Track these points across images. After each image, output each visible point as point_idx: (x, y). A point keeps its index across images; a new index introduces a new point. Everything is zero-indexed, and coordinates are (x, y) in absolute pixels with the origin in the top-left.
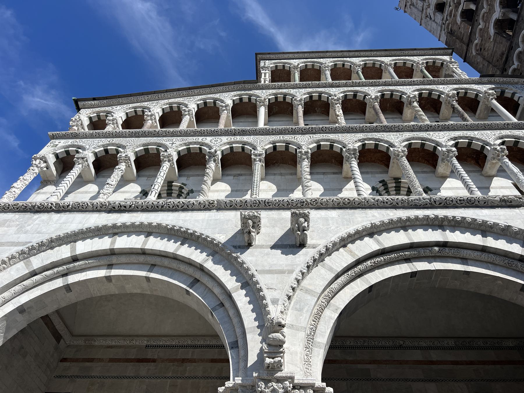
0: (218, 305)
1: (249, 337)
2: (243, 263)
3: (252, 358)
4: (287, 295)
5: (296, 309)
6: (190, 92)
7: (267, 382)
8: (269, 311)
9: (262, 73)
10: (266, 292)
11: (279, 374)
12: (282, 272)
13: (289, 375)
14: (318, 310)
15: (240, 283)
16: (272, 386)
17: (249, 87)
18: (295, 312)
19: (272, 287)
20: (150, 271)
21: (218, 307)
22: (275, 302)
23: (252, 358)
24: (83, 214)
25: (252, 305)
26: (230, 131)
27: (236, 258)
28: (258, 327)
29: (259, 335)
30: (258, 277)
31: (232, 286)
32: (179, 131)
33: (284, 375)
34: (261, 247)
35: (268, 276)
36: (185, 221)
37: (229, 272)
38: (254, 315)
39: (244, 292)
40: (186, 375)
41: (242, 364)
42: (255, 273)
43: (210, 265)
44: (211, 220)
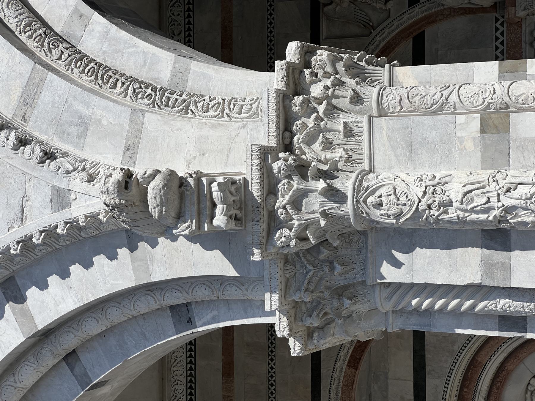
0: (72, 369)
4: (42, 162)
5: (83, 135)
8: (86, 217)
11: (255, 189)
13: (256, 161)
14: (82, 72)
15: (7, 307)
16: (284, 208)
18: (89, 139)
19: (18, 208)
21: (77, 370)
28: (133, 248)
29: (154, 244)
31: (16, 329)
33: (257, 174)
38: (100, 260)
39: (32, 293)
41: (233, 293)
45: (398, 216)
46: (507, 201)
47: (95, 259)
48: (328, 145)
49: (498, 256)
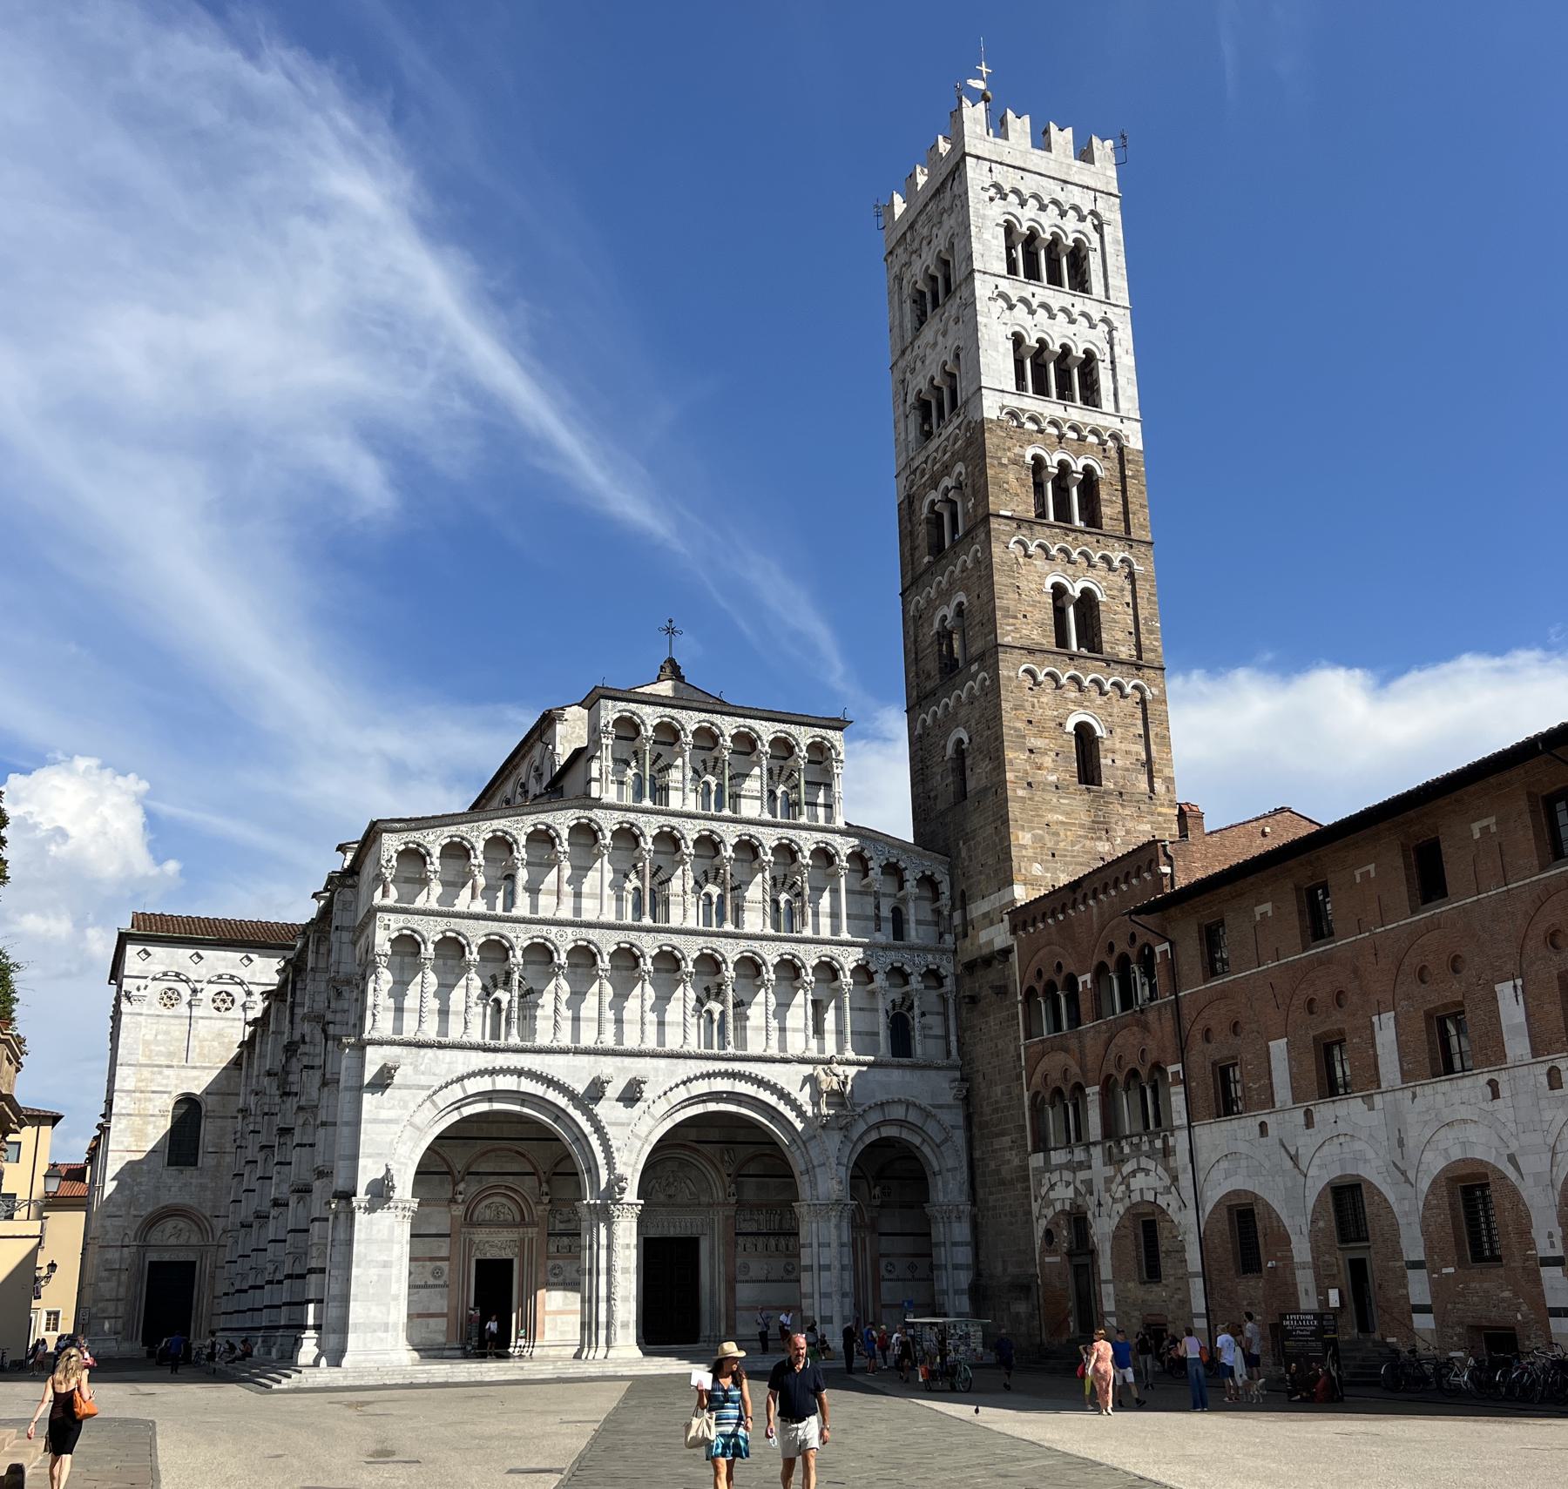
1: (601, 1171)
2: (597, 1115)
3: (603, 1185)
7: (615, 1205)
12: (622, 1124)
20: (522, 1105)
23: (603, 1185)
34: (609, 1099)
35: (614, 1128)
36: (549, 1066)
39: (596, 1136)
41: (595, 1187)
42: (606, 1126)
43: (571, 1110)
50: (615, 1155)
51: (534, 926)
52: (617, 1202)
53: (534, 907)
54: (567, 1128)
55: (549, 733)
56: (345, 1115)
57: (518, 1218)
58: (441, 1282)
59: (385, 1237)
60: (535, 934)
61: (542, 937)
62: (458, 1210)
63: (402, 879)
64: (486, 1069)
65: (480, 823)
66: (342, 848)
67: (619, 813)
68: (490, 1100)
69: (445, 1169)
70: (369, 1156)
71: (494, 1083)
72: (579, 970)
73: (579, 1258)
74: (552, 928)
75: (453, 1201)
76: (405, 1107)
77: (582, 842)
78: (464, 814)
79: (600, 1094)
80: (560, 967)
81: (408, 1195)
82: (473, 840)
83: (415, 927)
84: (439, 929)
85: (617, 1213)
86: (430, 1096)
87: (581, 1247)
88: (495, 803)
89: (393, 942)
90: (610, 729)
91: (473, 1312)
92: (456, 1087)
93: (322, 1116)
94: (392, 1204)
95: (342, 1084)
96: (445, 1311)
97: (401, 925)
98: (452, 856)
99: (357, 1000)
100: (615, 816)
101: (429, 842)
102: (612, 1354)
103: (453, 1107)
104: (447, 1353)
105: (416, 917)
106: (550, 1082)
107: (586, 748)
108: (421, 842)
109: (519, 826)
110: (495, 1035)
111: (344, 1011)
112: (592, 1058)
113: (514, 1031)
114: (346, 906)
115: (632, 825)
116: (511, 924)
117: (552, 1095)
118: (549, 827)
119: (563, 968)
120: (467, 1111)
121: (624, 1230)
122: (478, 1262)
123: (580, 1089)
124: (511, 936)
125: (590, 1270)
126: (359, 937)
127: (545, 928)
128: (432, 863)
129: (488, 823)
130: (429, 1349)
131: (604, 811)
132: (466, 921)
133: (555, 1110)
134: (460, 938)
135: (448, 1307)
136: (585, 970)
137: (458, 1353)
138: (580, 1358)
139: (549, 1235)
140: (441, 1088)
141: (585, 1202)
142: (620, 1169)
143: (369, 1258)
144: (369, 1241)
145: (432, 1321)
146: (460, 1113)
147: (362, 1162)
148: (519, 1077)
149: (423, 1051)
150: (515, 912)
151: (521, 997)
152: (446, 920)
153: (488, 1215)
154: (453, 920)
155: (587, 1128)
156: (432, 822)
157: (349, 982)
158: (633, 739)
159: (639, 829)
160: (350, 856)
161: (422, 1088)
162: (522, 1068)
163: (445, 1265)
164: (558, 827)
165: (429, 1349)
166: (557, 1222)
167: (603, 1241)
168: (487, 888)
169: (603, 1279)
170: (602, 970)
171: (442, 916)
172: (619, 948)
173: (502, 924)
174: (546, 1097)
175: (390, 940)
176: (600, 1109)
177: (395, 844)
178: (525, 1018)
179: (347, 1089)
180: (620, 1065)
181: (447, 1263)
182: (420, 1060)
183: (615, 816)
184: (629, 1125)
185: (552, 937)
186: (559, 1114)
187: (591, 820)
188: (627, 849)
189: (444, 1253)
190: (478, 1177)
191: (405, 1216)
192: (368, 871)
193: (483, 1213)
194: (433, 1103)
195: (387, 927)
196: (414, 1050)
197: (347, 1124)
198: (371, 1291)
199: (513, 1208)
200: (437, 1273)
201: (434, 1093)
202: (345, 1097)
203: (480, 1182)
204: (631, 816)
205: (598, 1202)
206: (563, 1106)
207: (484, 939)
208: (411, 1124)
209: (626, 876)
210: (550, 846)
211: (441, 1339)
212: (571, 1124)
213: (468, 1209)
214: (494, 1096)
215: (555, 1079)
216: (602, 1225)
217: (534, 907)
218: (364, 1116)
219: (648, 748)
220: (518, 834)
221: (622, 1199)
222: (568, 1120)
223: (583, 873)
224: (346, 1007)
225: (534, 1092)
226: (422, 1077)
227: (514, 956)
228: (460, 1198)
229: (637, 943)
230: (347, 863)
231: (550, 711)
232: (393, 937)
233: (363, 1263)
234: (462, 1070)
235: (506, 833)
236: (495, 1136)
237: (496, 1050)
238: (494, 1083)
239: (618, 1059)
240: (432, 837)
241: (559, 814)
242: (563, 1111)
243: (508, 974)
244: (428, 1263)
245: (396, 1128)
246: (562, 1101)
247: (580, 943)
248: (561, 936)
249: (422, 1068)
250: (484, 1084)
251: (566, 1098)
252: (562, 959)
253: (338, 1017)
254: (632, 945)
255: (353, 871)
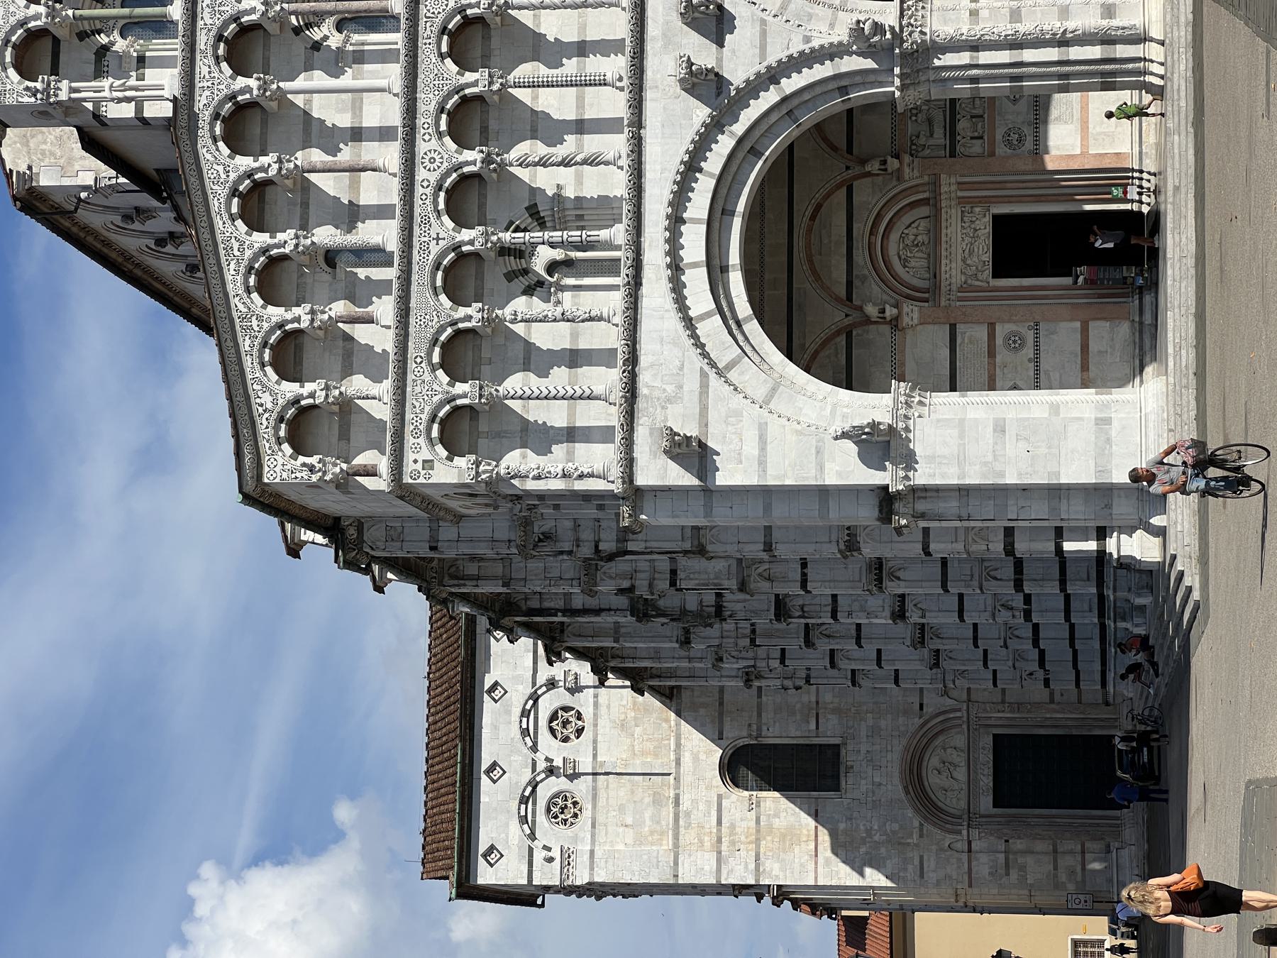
0: (790, 117)
1: (844, 69)
2: (748, 81)
3: (869, 64)
6: (207, 248)
7: (902, 41)
9: (70, 98)
10: (794, 50)
11: (897, 29)
12: (764, 34)
13: (898, 20)
15: (771, 87)
17: (186, 117)
18: (813, 21)
19: (786, 44)
20: (733, 213)
21: (793, 118)
22: (807, 40)
23: (869, 64)
24: (641, 322)
25: (803, 70)
26: (407, 135)
27: (737, 89)
29: (842, 58)
30: (772, 60)
32: (403, 231)
33: (898, 25)
34: (719, 60)
37: (752, 102)
39: (784, 81)
40: (757, 267)
41: (872, 78)
42: (765, 64)
43: (739, 128)
44: (663, 134)
45: (945, 39)
46: (982, 33)
47: (803, 70)
48: (916, 20)
49: (975, 54)
50: (815, 44)
51: (417, 211)
52: (898, 37)
53: (382, 212)
54: (770, 133)
55: (58, 199)
56: (753, 516)
57: (925, 211)
58: (1030, 336)
59: (955, 432)
60: (430, 208)
61: (436, 196)
62: (911, 313)
63: (343, 443)
64: (671, 280)
65: (235, 314)
66: (294, 550)
67: (198, 63)
68: (725, 269)
69: (842, 340)
70: (821, 468)
71: (695, 265)
72: (493, 125)
73: (992, 100)
74: (419, 178)
75: (895, 323)
76: (738, 414)
77: (258, 131)
78: (219, 345)
79: (711, 76)
80: (487, 160)
81: (886, 399)
82: (266, 326)
83: (425, 417)
84: (427, 377)
85: (916, 35)
86: (720, 373)
87: (975, 98)
88: (197, 290)
89: (453, 452)
90: (39, 85)
91: (1081, 279)
92: (702, 328)
93: (754, 550)
94: (901, 425)
95: (701, 522)
96: (1078, 324)
97: (422, 441)
98: (298, 362)
99: (556, 507)
100: (205, 70)
101: (275, 402)
102: (1156, 33)
103: (736, 332)
104: (1148, 319)
105: (409, 416)
106: (691, 167)
107: (80, 130)
108: (275, 415)
109: (236, 245)
110: (610, 267)
111: (577, 526)
112: (649, 95)
113: (604, 234)
114: (395, 536)
115: (220, 38)
116: (415, 252)
117: (714, 162)
118: (234, 192)
119: (489, 154)
120: (743, 307)
121: (945, 22)
122: (997, 274)
123: (701, 113)
124: (435, 249)
125: (1014, 78)
126: (448, 510)
127: (419, 191)
128: (312, 395)
129: (235, 301)
130: (1141, 348)
131: (197, 92)
132: (412, 330)
133: (740, 155)
134: (442, 338)
135: (1072, 320)
136: (493, 114)
137: (1148, 299)
138: (1162, 87)
139: (953, 155)
140: (705, 355)
141: (897, 94)
142: (841, 34)
143: (990, 458)
144: (961, 460)
145: (1093, 347)
146: (747, 319)
147: (831, 480)
148: (684, 222)
149: (643, 390)
150: (393, 245)
151: (542, 225)
152: (411, 365)
153: (918, 262)
154: (412, 353)
155: (769, 98)
156: (239, 398)
157: (526, 523)
158: (56, 42)
159: (225, 25)
160: (307, 535)
161: (704, 386)
162: (668, 217)
163: (1001, 330)
164: (233, 176)
165: (1141, 348)
166: (931, 142)
167: (964, 58)
168: (352, 298)
169: (1029, 55)
170: (491, 83)
171: (405, 373)
172: (450, 54)
173: (415, 268)
174: (717, 172)
175: (450, 459)
176: (738, 71)
177: (280, 461)
178: (580, 217)
179: (708, 512)
180: (660, 44)
181: (998, 328)
182: (656, 393)
183: (205, 70)
184: (763, 22)
185: (433, 177)
186: (747, 148)
187: (216, 116)
188: (266, 47)
189: (981, 333)
190: (856, 282)
191: (921, 403)
192: (333, 504)
193: (914, 273)
194: (730, 366)
195: (428, 464)
196: (641, 404)
197: (767, 508)
198: (1043, 450)
199: (907, 219)
200: (1015, 342)
201: (713, 364)
202: (722, 516)
203: (864, 279)
204: (204, 40)
205: (897, 70)
206: (732, 143)
207: (443, 298)
208: (767, 401)
209: (317, 46)
210: (269, 189)
211: (1124, 329)
212: (764, 127)
213: (908, 297)
214: (716, 262)
215: (686, 158)
216: (937, 63)
217: (382, 212)
218: (753, 481)
219: (70, 12)
220: (251, 246)
221: (892, 28)
222: (757, 133)
223: (315, 128)
224: (569, 524)
225: (710, 195)
226: (686, 388)
227: (471, 242)
228: (890, 312)
229: (439, 21)
230: (319, 539)
231: (15, 198)
232: (444, 453)
233: (998, 467)
234: (673, 322)
235: (250, 269)
236: (785, 259)
237: (637, 265)
238: (695, 265)
239: (649, 47)
240: (266, 399)
241: (208, 175)
242: (740, 141)
243: (505, 251)
244: (998, 359)
245: (774, 425)
246: (724, 145)
247: (443, 127)
248: (432, 160)
249: (670, 389)
250: (697, 282)
251: (720, 137)
252: (473, 157)
253: (587, 535)
254: (443, 30)
255: (332, 528)
